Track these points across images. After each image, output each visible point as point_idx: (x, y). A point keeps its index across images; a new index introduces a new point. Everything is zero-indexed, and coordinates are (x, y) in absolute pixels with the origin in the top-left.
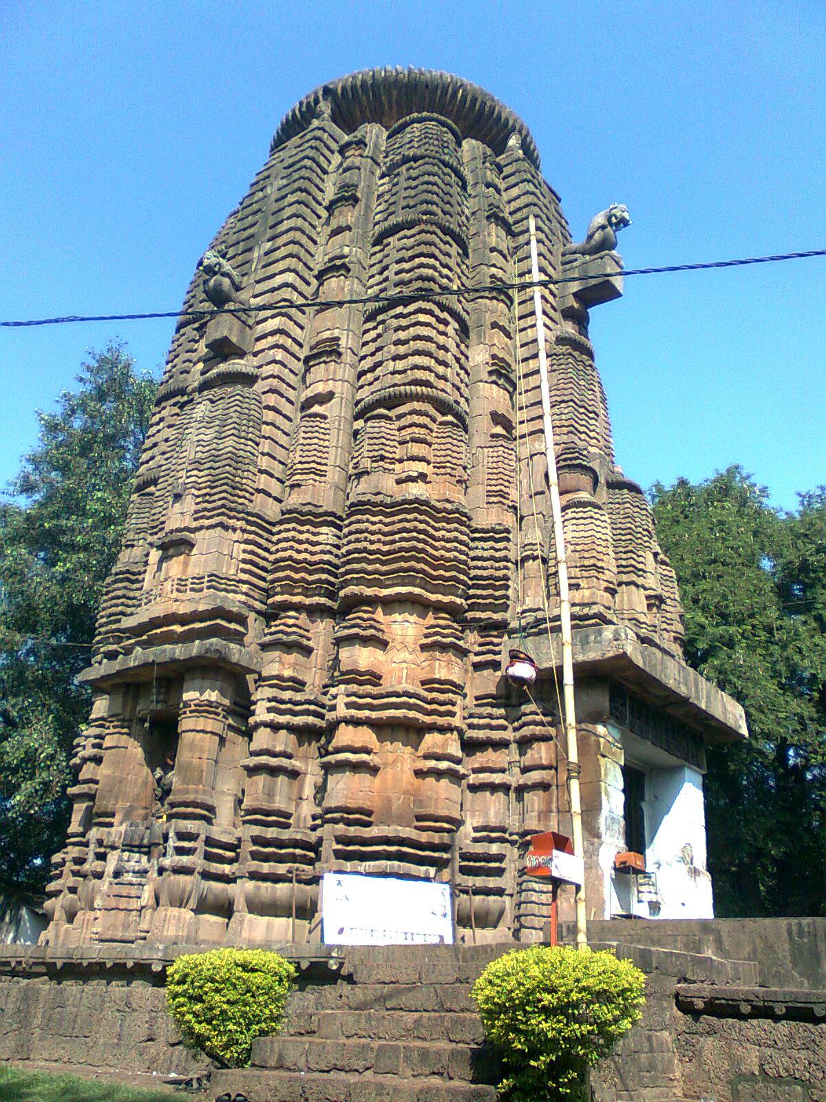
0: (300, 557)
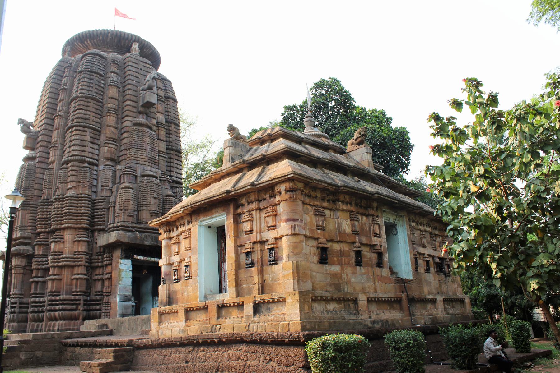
0: (44, 216)
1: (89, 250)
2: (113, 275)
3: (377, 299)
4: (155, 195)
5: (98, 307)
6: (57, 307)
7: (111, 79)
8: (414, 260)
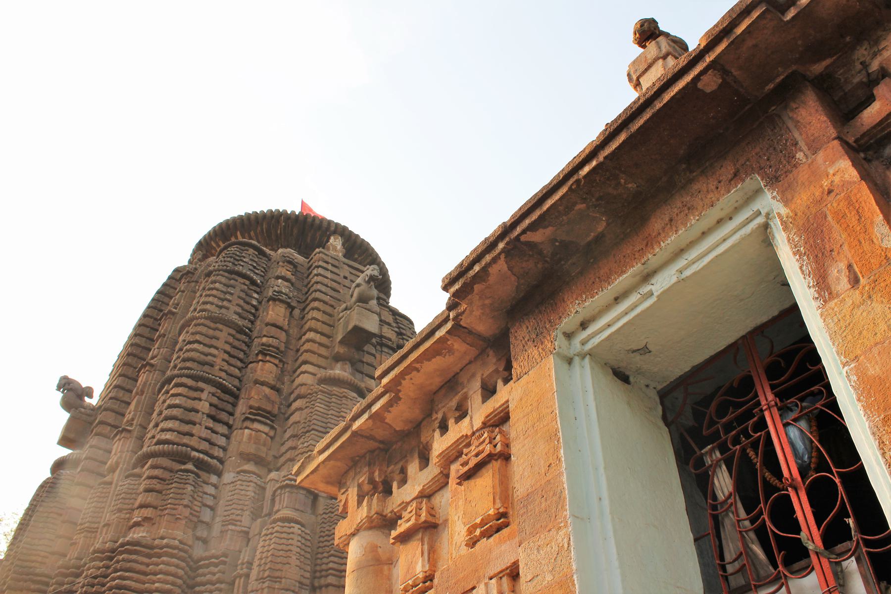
7: (276, 288)
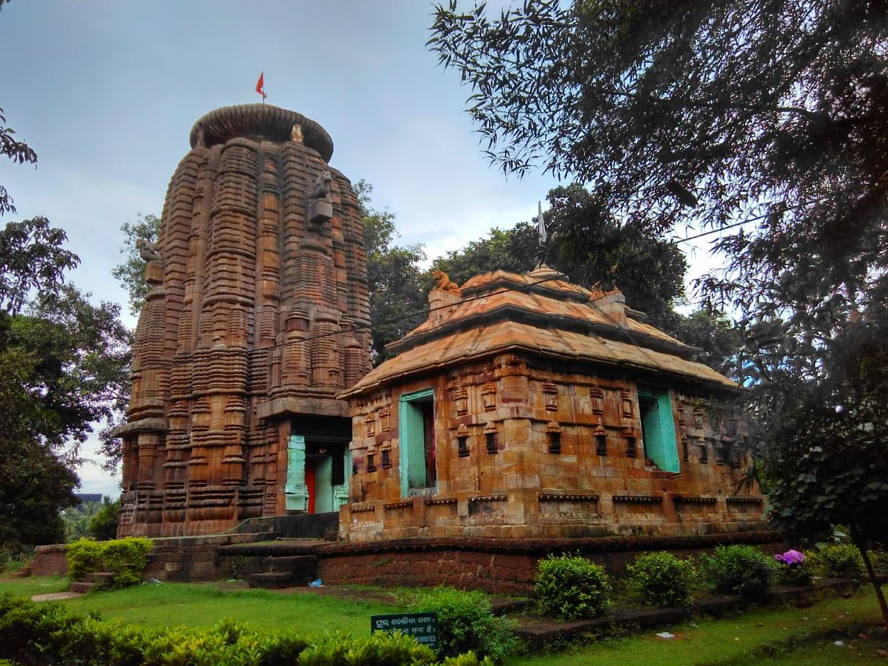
1: (245, 422)
2: (280, 456)
3: (626, 499)
4: (335, 346)
5: (258, 501)
6: (203, 502)
8: (681, 446)
